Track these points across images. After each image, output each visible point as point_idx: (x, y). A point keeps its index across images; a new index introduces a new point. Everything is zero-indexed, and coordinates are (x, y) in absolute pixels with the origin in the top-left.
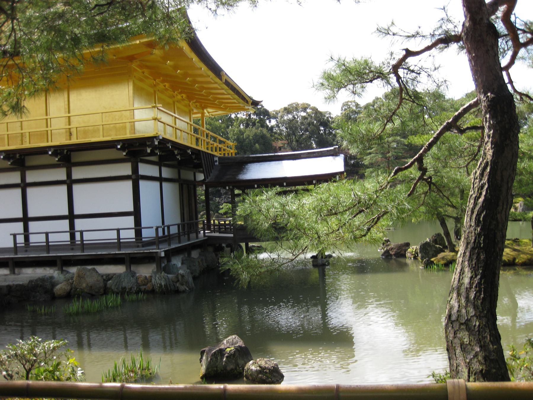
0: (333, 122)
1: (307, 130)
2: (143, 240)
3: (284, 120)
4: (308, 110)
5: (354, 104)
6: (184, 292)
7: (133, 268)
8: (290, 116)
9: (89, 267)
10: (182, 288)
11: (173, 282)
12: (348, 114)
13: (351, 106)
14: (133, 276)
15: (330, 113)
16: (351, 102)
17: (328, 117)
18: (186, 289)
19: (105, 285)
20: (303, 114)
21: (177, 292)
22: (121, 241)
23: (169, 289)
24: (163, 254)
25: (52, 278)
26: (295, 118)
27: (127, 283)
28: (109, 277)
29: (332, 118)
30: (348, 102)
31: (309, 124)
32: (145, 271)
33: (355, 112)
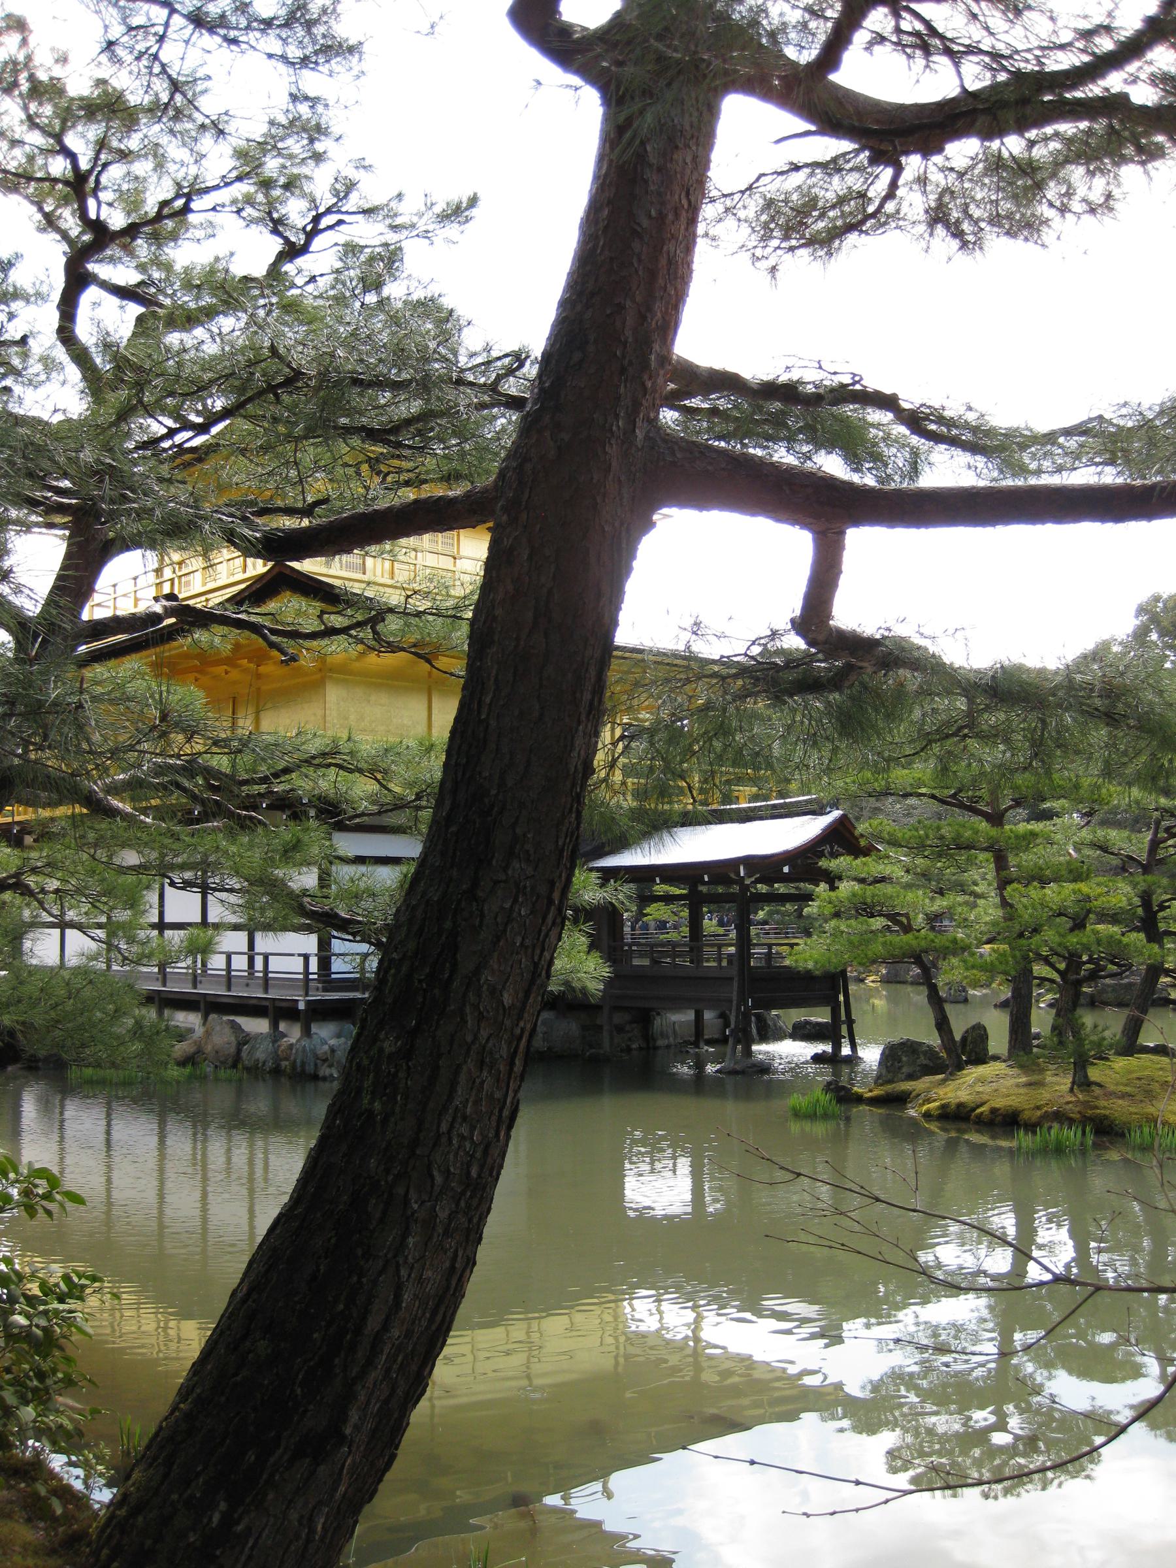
2: (333, 976)
6: (324, 1079)
7: (282, 1026)
9: (225, 1018)
10: (325, 1071)
11: (317, 1057)
14: (274, 1042)
18: (331, 1075)
19: (239, 1051)
21: (315, 1077)
22: (270, 975)
23: (299, 1069)
24: (301, 1006)
25: (191, 1031)
27: (262, 1053)
28: (245, 1040)
32: (293, 1033)
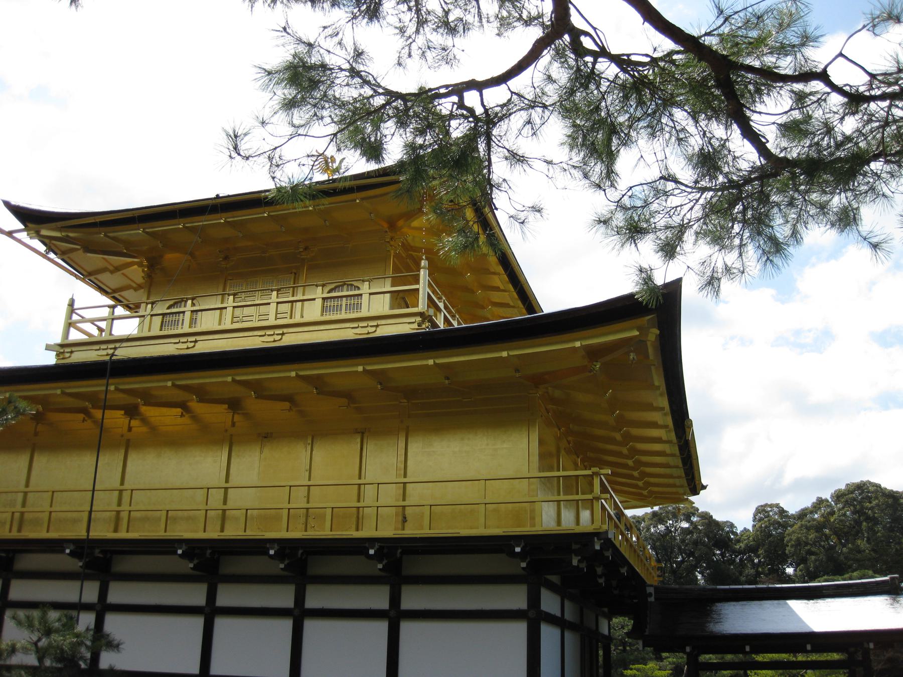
0: (738, 541)
1: (691, 554)
3: (652, 534)
4: (695, 519)
5: (775, 509)
8: (661, 527)
12: (766, 527)
13: (771, 513)
15: (732, 525)
16: (771, 506)
17: (728, 532)
20: (685, 525)
26: (671, 531)
29: (735, 534)
30: (766, 505)
31: (696, 543)
33: (779, 522)
